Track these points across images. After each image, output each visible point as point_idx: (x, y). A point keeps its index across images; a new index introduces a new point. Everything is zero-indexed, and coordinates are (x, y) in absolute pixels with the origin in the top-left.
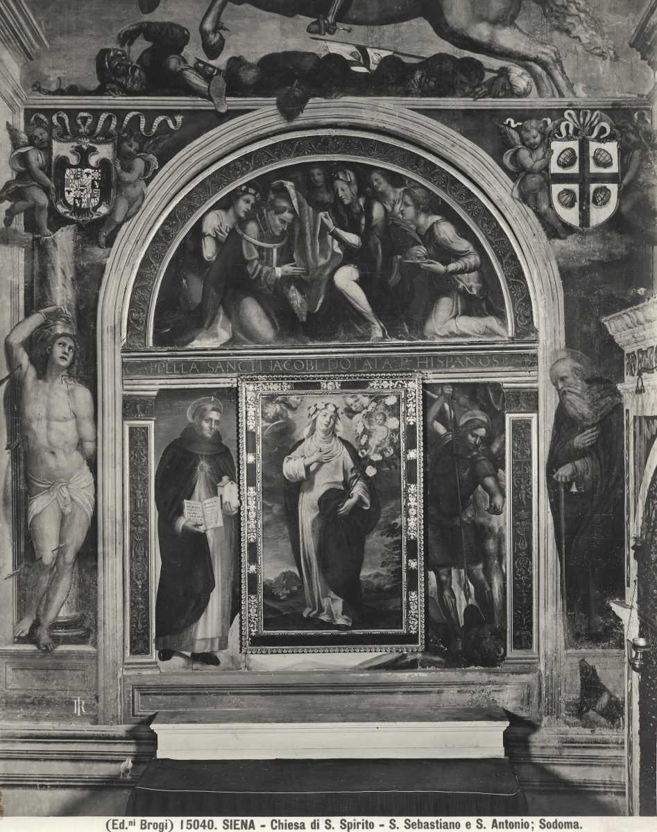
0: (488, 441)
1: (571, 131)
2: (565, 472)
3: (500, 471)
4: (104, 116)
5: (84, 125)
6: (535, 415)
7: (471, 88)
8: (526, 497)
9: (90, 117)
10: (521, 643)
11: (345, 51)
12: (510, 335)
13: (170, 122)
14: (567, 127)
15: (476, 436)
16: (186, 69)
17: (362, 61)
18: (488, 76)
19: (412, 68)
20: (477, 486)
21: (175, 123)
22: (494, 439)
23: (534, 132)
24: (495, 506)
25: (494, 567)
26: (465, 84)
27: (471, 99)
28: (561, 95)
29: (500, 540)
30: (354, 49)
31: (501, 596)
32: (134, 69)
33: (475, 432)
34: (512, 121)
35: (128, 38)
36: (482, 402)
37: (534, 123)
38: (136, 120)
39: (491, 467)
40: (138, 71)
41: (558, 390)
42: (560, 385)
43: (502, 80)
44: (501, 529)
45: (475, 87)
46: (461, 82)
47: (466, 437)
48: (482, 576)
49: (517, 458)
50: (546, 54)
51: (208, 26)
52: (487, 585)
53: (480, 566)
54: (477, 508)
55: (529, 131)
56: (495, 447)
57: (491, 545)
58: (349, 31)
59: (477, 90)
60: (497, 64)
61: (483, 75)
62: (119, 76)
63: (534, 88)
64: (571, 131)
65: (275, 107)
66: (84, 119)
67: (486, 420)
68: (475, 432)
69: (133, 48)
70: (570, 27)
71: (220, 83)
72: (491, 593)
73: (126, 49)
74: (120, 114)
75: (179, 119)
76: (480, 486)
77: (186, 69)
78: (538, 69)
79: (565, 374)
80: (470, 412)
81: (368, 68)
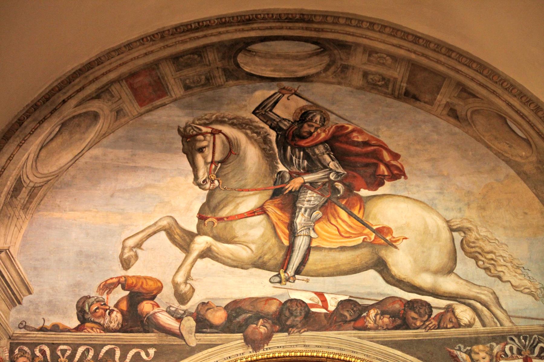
1: (515, 351)
4: (81, 350)
5: (63, 355)
7: (422, 321)
9: (69, 350)
11: (307, 298)
13: (143, 354)
14: (511, 349)
16: (158, 312)
17: (320, 304)
18: (435, 312)
19: (367, 308)
21: (147, 354)
23: (482, 354)
26: (416, 319)
27: (424, 331)
28: (501, 325)
30: (314, 295)
32: (111, 311)
34: (462, 346)
35: (108, 287)
37: (481, 347)
38: (110, 353)
40: (115, 313)
43: (449, 315)
45: (425, 322)
46: (413, 318)
50: (484, 294)
51: (180, 279)
55: (478, 353)
58: (307, 281)
59: (427, 323)
60: (443, 303)
61: (431, 312)
62: (99, 317)
63: (477, 320)
64: (515, 351)
65: (243, 341)
66: (64, 352)
69: (111, 296)
70: (501, 274)
71: (190, 323)
73: (105, 296)
74: (97, 348)
75: (152, 351)
77: (158, 312)
78: (478, 305)
81: (327, 309)
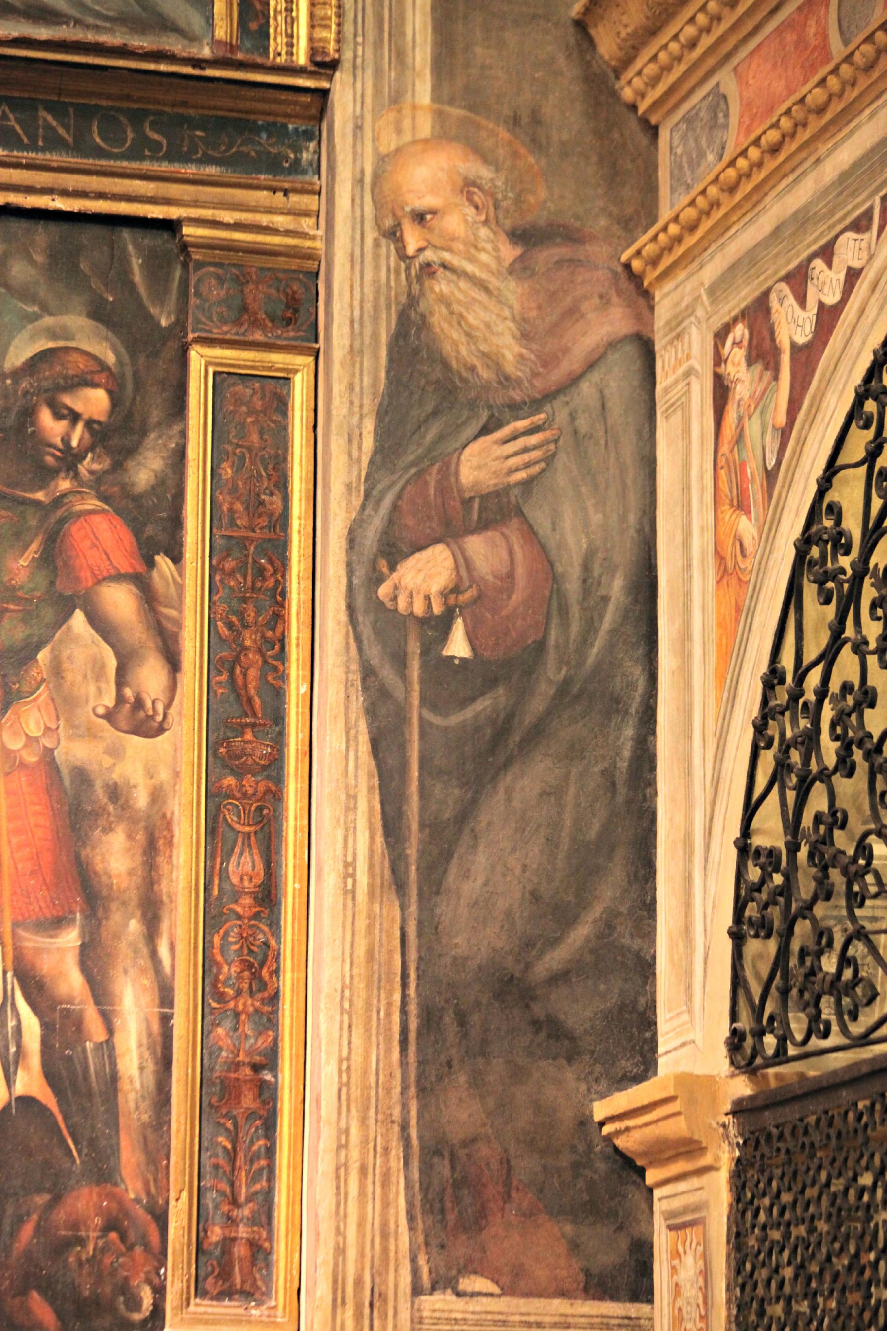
0: (117, 437)
2: (424, 576)
3: (163, 562)
6: (304, 361)
8: (263, 677)
10: (225, 1274)
12: (221, 32)
15: (75, 417)
20: (69, 614)
22: (144, 433)
24: (139, 703)
25: (123, 947)
29: (154, 844)
31: (150, 1066)
33: (67, 400)
36: (95, 283)
39: (128, 538)
41: (402, 256)
42: (412, 241)
44: (157, 796)
47: (29, 414)
48: (72, 982)
49: (232, 523)
52: (91, 1015)
53: (70, 938)
54: (65, 704)
56: (145, 472)
57: (115, 856)
67: (111, 359)
68: (67, 400)
72: (108, 1048)
76: (78, 619)
79: (428, 201)
80: (48, 321)
